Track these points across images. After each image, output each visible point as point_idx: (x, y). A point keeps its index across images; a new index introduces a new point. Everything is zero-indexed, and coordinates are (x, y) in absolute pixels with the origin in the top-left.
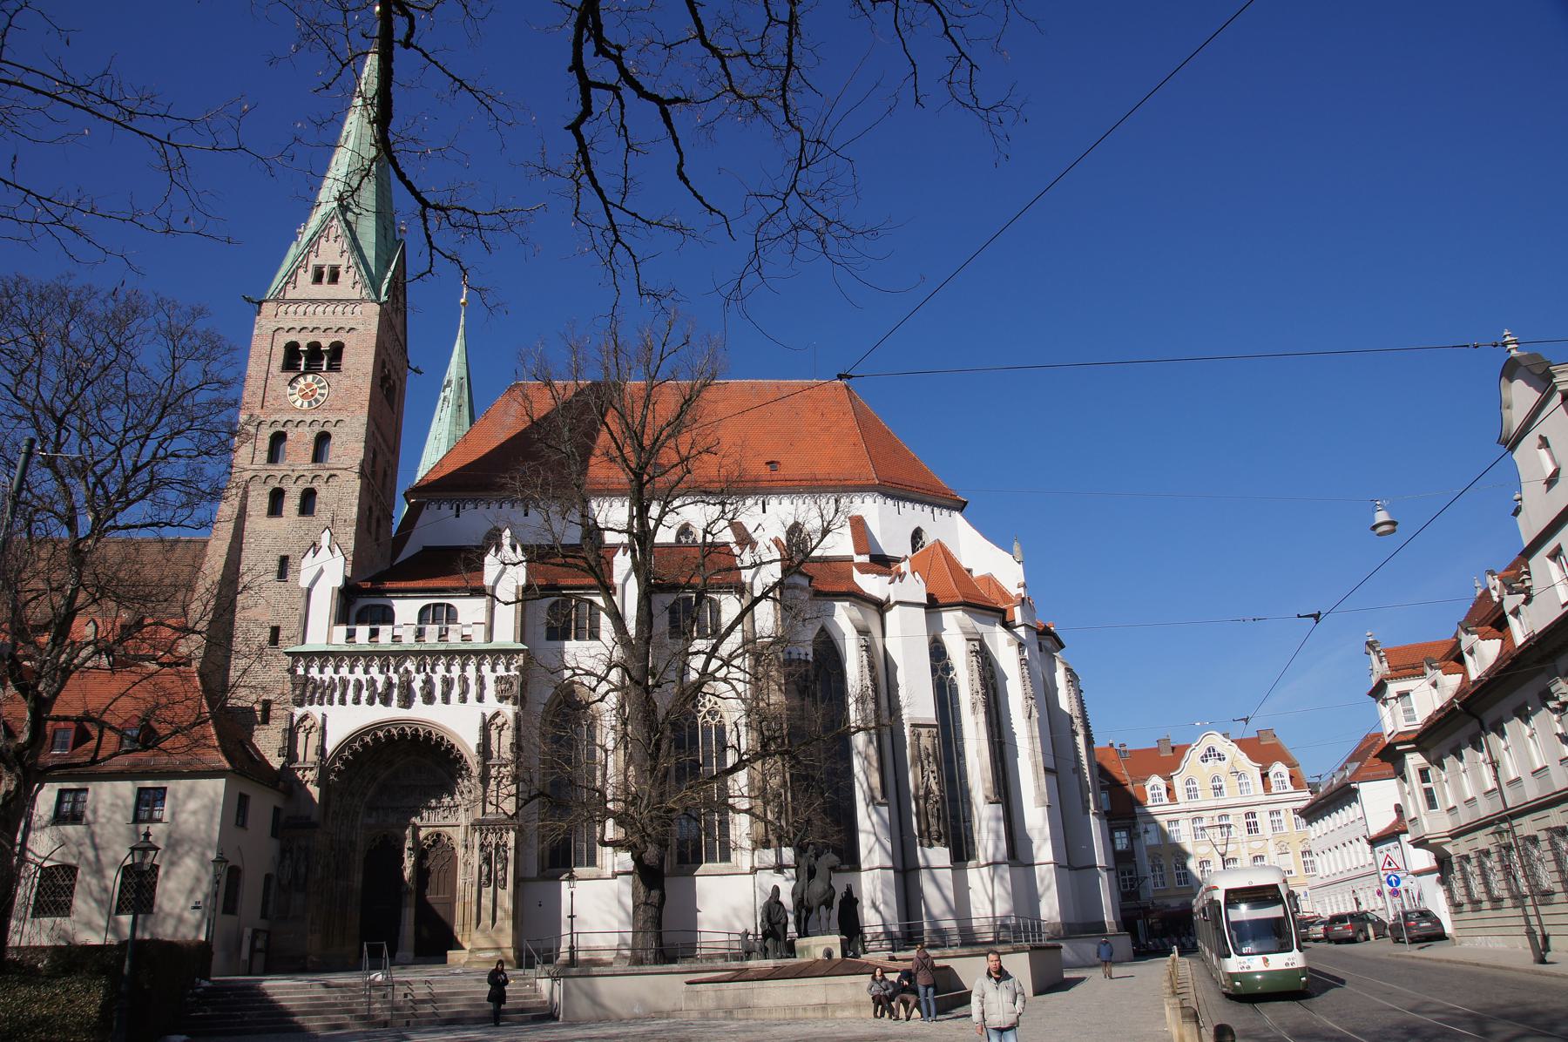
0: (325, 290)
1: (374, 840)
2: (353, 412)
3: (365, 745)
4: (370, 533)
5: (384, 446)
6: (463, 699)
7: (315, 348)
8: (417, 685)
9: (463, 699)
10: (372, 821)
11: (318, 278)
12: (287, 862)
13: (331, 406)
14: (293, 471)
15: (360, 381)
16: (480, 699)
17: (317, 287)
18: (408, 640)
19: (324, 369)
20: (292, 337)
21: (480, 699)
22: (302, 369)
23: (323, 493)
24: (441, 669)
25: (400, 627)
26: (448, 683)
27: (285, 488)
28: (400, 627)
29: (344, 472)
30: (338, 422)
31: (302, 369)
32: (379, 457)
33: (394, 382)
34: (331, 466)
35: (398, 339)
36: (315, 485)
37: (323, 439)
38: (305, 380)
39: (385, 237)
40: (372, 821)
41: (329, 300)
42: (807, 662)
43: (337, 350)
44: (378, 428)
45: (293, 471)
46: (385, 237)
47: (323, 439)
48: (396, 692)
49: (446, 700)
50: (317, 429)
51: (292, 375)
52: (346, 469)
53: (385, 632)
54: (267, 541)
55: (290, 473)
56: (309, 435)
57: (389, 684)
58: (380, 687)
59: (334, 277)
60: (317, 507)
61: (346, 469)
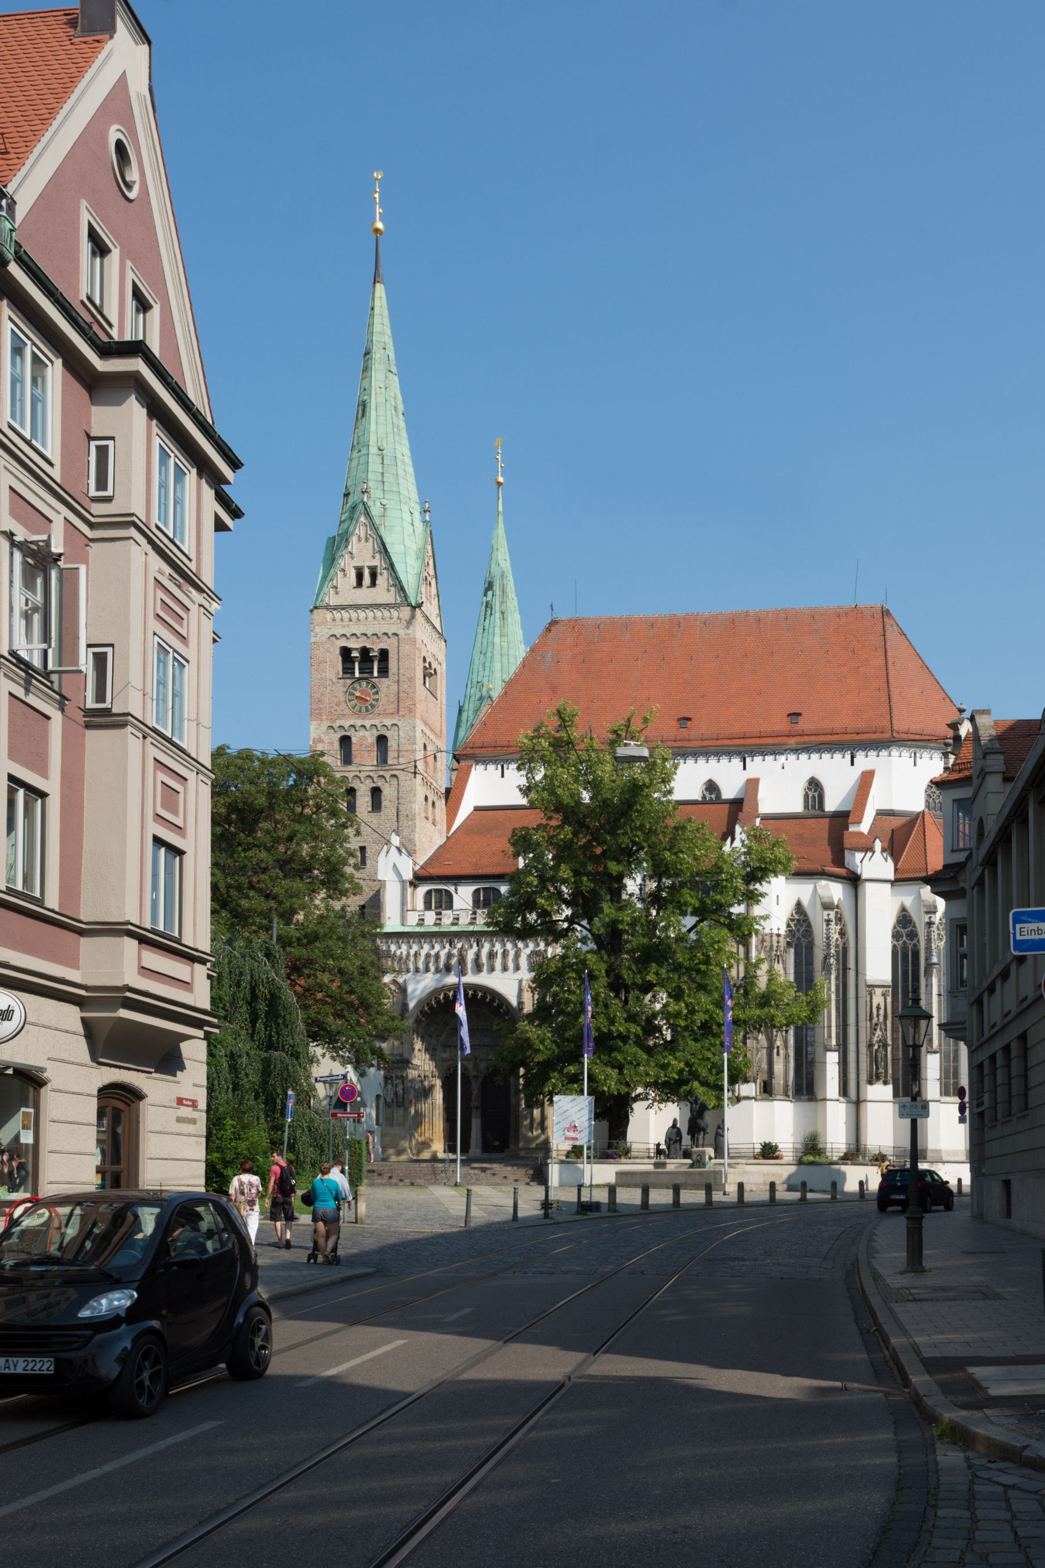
0: (365, 595)
1: (449, 1069)
2: (403, 716)
3: (438, 1001)
4: (427, 818)
5: (432, 737)
6: (505, 969)
7: (365, 651)
8: (470, 955)
11: (359, 583)
12: (390, 1087)
13: (384, 711)
15: (406, 686)
17: (358, 591)
18: (465, 920)
19: (376, 674)
20: (343, 643)
21: (517, 968)
22: (357, 675)
23: (388, 792)
24: (487, 946)
25: (457, 910)
26: (492, 955)
27: (356, 787)
28: (457, 910)
29: (401, 772)
30: (393, 725)
31: (357, 675)
32: (429, 748)
33: (435, 670)
35: (434, 628)
36: (380, 783)
37: (382, 740)
38: (361, 686)
39: (413, 525)
41: (371, 605)
42: (778, 935)
43: (384, 654)
44: (426, 724)
46: (413, 525)
47: (382, 740)
49: (492, 969)
50: (376, 733)
51: (349, 682)
52: (403, 770)
53: (447, 917)
55: (358, 774)
56: (371, 737)
57: (449, 956)
59: (373, 584)
60: (383, 804)
61: (403, 770)
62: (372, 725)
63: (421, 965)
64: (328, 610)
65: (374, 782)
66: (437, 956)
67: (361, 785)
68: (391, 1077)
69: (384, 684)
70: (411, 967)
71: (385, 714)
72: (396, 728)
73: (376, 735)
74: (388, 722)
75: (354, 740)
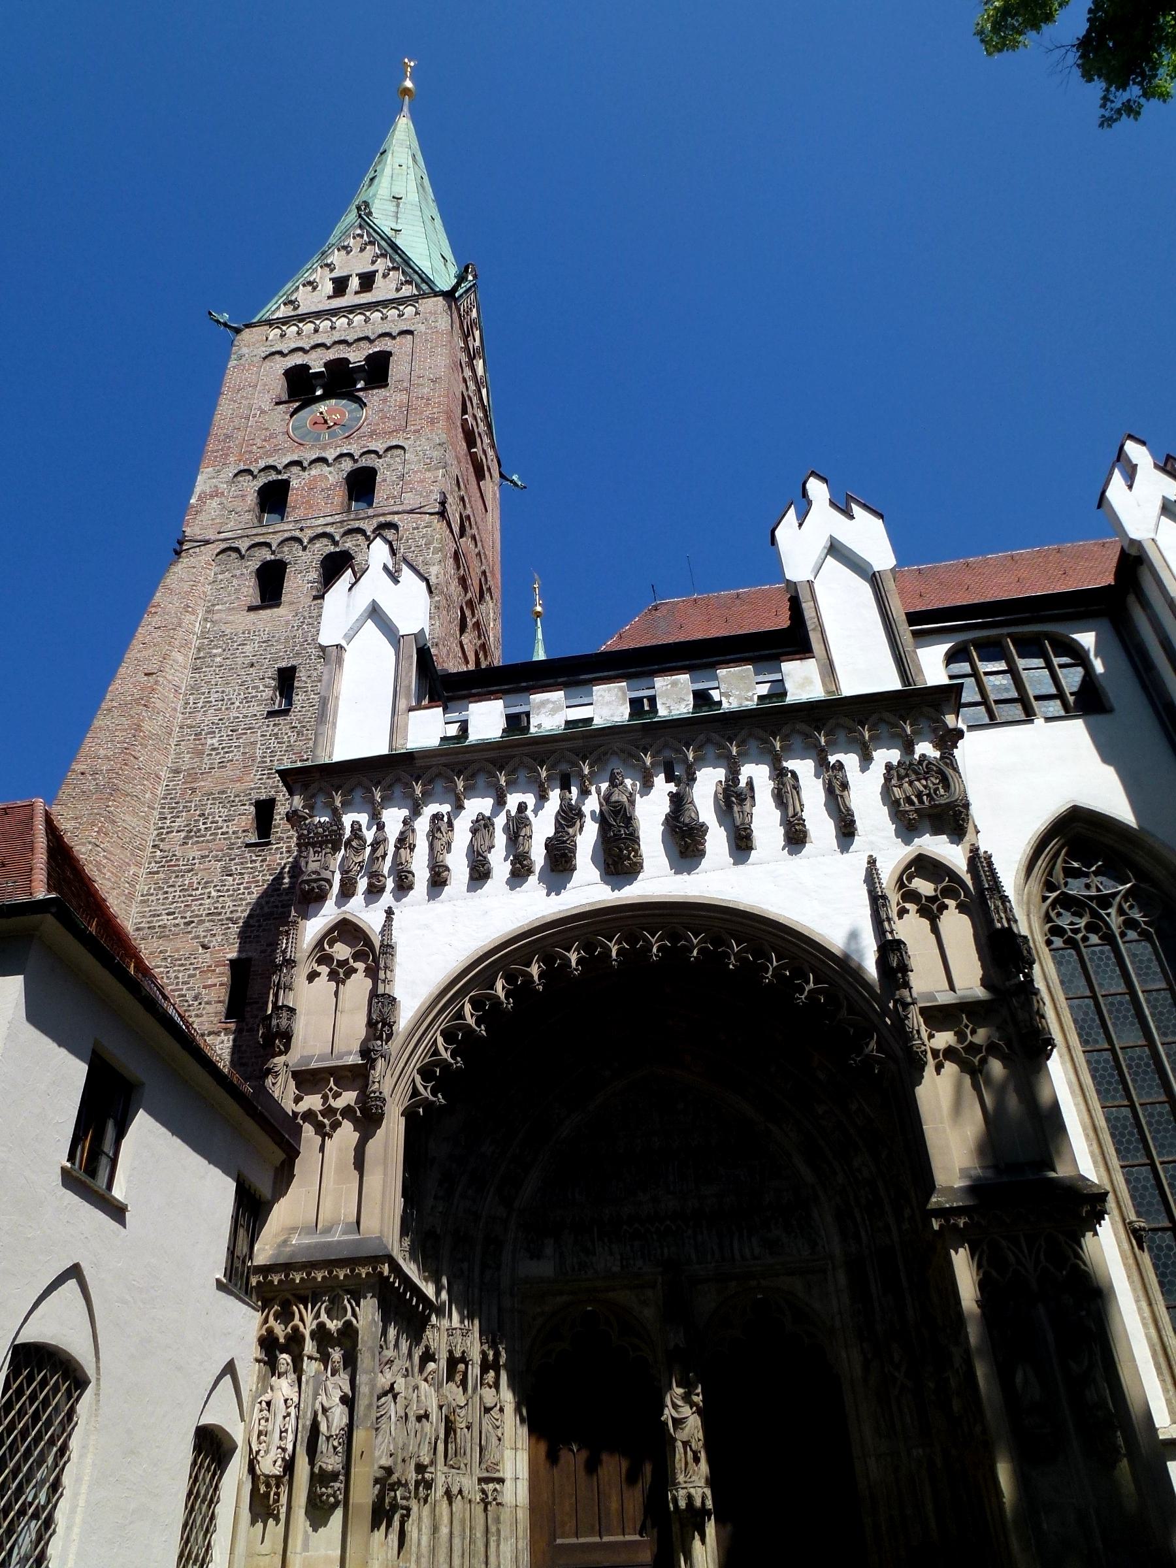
9: (796, 837)
10: (544, 1268)
14: (302, 529)
16: (846, 830)
34: (380, 511)
40: (544, 1268)
45: (302, 529)
48: (587, 838)
50: (347, 465)
54: (248, 649)
56: (334, 476)
57: (569, 817)
58: (543, 826)
62: (342, 455)
63: (458, 863)
64: (271, 325)
65: (336, 543)
66: (518, 828)
67: (301, 553)
68: (295, 1339)
69: (374, 398)
70: (421, 874)
71: (373, 434)
72: (400, 451)
73: (349, 469)
74: (380, 447)
75: (294, 483)
